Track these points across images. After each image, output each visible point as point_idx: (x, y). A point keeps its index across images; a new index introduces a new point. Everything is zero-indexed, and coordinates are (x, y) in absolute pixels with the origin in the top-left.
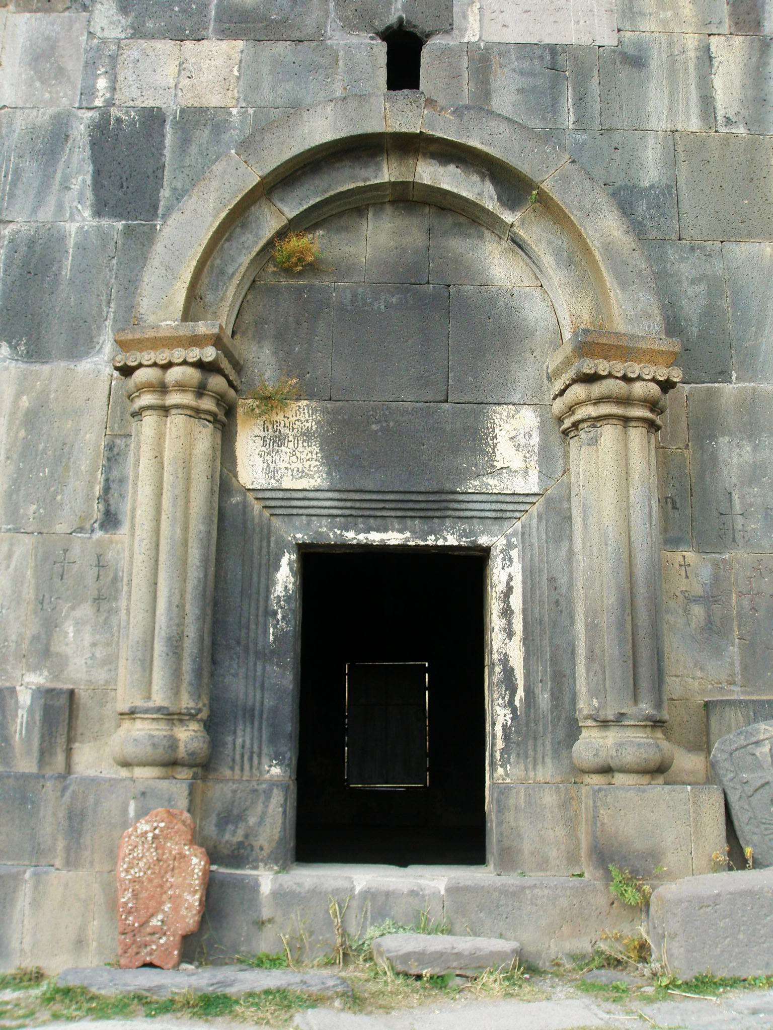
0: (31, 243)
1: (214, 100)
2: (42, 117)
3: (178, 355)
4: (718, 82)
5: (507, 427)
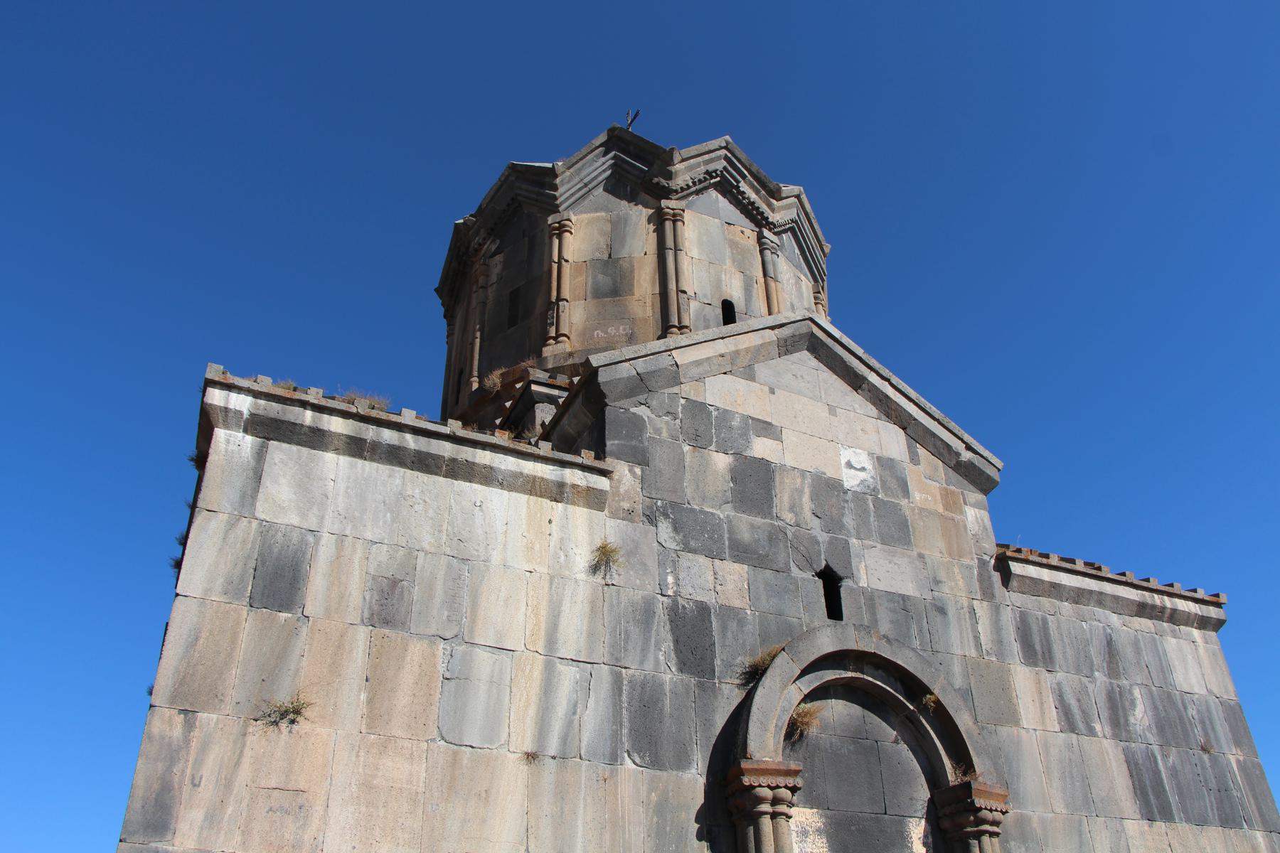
0: (643, 685)
1: (737, 603)
2: (638, 596)
3: (781, 781)
4: (980, 629)
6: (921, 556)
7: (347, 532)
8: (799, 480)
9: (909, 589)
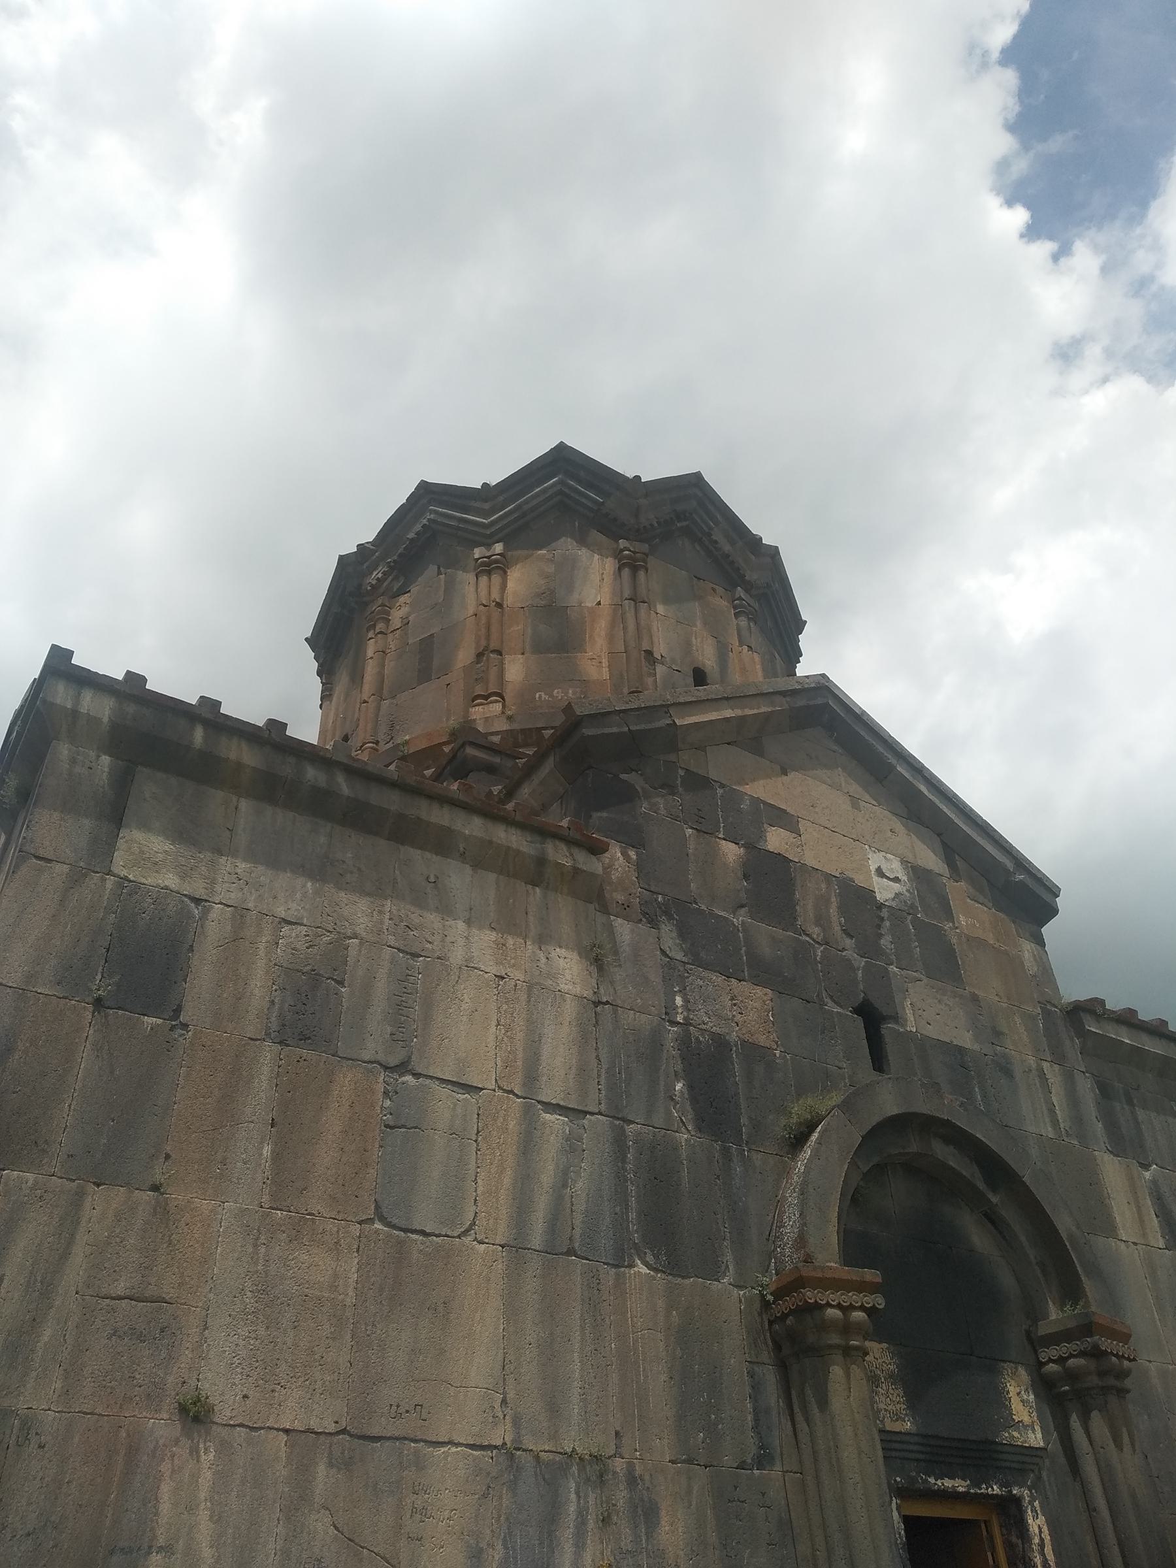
1: (762, 1040)
3: (854, 1298)
4: (1055, 1100)
5: (1013, 1382)
6: (975, 999)
7: (251, 905)
8: (823, 886)
9: (966, 1040)
